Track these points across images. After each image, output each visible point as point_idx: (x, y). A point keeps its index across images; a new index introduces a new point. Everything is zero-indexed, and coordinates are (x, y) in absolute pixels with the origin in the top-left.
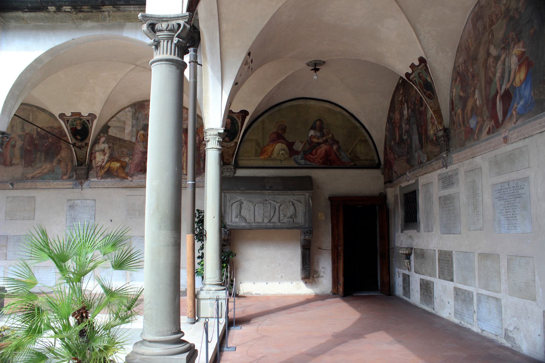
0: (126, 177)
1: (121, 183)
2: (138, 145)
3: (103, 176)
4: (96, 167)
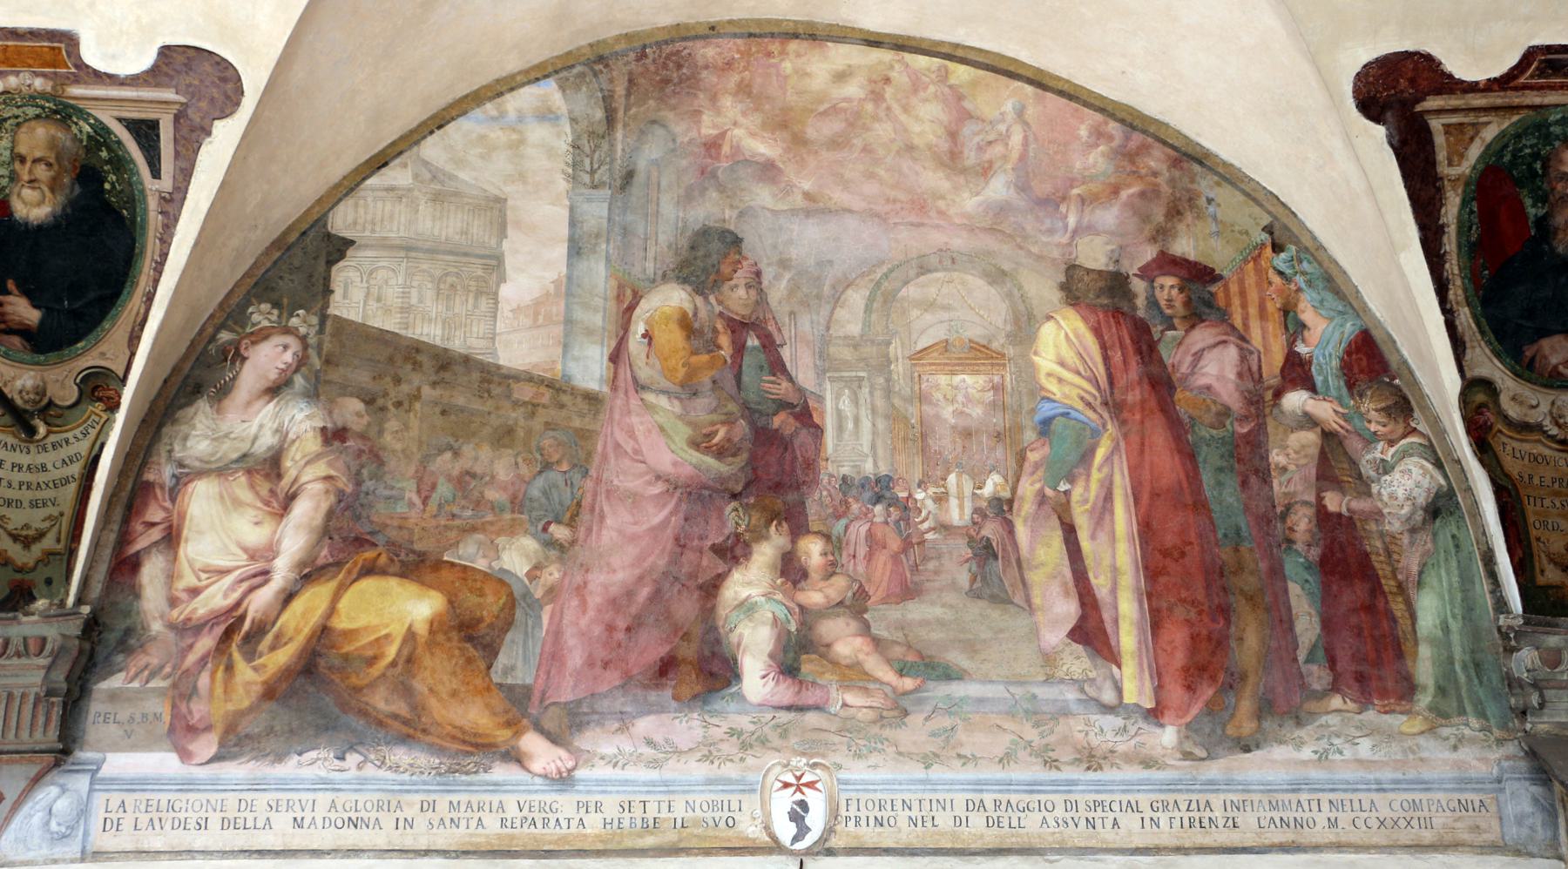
0: (503, 735)
1: (443, 801)
2: (635, 420)
3: (246, 726)
4: (172, 626)
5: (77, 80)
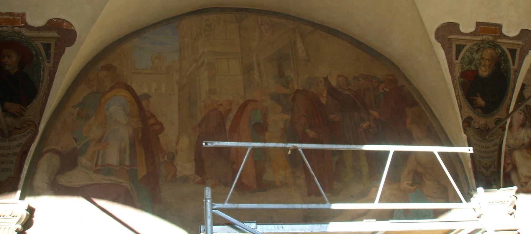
5: (499, 37)
